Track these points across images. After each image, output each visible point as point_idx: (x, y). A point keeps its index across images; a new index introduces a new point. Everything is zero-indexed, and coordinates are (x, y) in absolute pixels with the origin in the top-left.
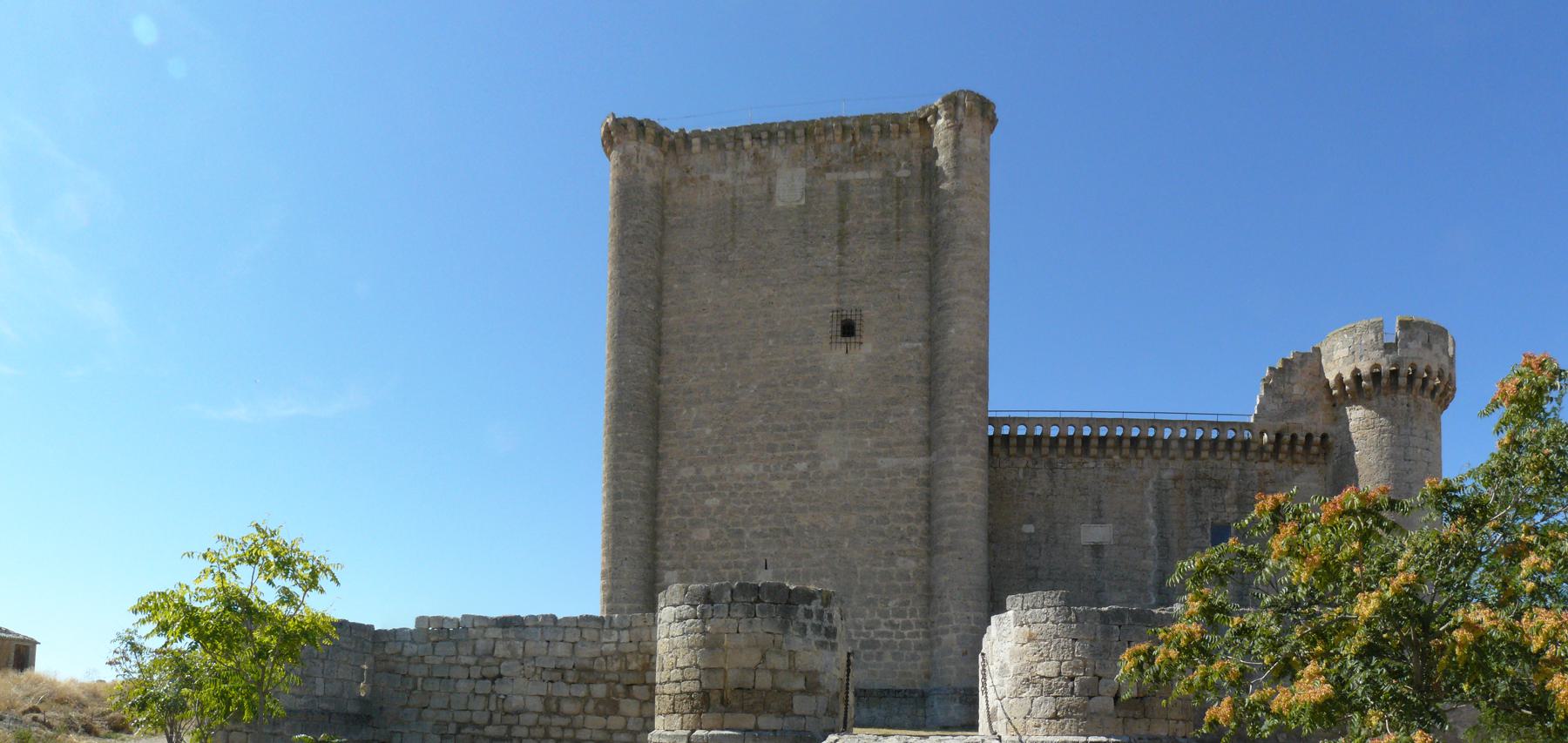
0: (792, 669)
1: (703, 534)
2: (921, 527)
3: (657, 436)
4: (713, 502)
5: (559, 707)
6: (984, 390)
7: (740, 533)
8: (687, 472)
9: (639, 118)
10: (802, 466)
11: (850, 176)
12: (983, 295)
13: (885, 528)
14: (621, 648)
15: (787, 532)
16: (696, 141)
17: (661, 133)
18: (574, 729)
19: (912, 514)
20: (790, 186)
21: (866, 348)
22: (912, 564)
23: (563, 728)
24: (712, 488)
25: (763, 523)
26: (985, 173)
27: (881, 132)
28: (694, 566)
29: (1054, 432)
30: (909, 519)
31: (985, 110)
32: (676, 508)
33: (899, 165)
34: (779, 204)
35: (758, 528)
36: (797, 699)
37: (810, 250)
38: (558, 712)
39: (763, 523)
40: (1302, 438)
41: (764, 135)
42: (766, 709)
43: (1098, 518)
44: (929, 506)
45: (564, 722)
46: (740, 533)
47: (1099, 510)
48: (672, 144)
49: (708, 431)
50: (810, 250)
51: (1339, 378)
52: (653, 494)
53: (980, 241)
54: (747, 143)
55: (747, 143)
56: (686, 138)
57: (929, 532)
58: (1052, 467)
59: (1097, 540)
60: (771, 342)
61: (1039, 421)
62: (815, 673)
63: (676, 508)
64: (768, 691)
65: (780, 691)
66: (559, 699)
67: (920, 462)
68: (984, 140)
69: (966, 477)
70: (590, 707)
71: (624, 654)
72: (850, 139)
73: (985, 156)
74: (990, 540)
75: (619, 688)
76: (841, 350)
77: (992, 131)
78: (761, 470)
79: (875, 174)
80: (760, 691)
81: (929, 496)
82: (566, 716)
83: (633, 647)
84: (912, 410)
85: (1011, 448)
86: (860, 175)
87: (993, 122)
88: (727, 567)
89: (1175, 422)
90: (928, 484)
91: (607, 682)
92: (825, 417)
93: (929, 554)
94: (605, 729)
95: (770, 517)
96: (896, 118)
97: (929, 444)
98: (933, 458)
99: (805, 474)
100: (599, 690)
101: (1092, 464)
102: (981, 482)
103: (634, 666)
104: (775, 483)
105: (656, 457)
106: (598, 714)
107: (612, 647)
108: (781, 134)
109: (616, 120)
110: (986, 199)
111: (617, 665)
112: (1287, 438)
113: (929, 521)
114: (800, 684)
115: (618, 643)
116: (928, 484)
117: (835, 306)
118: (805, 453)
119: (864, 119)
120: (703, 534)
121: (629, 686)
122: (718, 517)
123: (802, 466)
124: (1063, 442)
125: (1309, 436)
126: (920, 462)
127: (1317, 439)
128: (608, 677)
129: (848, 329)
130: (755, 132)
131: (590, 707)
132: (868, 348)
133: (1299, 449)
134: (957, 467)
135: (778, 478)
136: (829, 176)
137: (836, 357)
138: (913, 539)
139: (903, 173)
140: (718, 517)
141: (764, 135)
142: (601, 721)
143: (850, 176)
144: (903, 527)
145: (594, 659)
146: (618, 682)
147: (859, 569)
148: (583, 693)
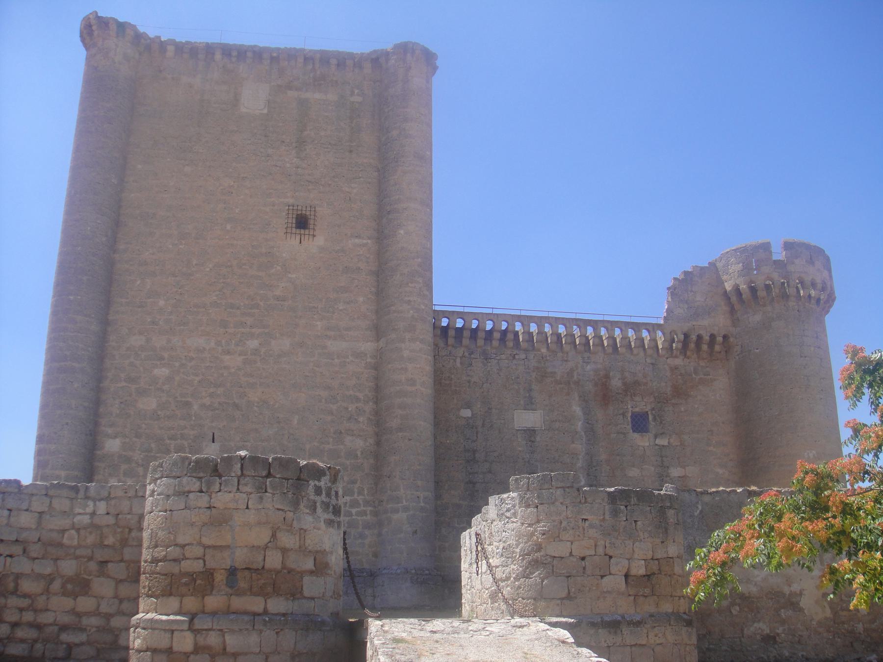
0: (303, 550)
1: (149, 404)
2: (369, 407)
3: (108, 304)
4: (162, 372)
5: (17, 585)
6: (428, 285)
7: (188, 404)
8: (137, 341)
9: (121, 20)
10: (253, 344)
11: (308, 95)
12: (428, 204)
13: (334, 407)
14: (97, 521)
15: (236, 406)
16: (171, 48)
17: (139, 37)
18: (35, 611)
19: (361, 396)
20: (254, 98)
21: (320, 240)
22: (359, 444)
23: (21, 610)
24: (162, 358)
25: (211, 395)
26: (428, 105)
27: (338, 65)
28: (138, 436)
29: (489, 326)
30: (358, 399)
31: (429, 58)
32: (123, 375)
33: (352, 94)
34: (244, 110)
35: (207, 401)
36: (307, 579)
37: (270, 151)
38: (15, 592)
39: (211, 395)
40: (707, 338)
41: (234, 53)
42: (276, 591)
43: (530, 404)
44: (377, 389)
45: (25, 603)
46: (188, 404)
47: (531, 398)
48: (147, 48)
49: (162, 303)
50: (270, 151)
51: (737, 290)
52: (100, 356)
53: (425, 159)
54: (218, 56)
55: (218, 56)
56: (162, 46)
57: (377, 413)
58: (486, 357)
59: (529, 425)
60: (228, 227)
61: (475, 316)
62: (324, 552)
63: (123, 375)
64: (278, 572)
65: (290, 571)
66: (18, 577)
67: (368, 347)
68: (428, 81)
69: (414, 365)
70: (56, 586)
71: (97, 527)
72: (310, 67)
73: (428, 92)
74: (436, 424)
75: (93, 566)
76: (294, 241)
77: (433, 75)
78: (213, 344)
79: (332, 97)
80: (270, 571)
81: (377, 378)
82: (25, 596)
83: (111, 520)
84: (361, 299)
85: (458, 339)
86: (317, 96)
87: (435, 68)
88: (173, 438)
89: (596, 322)
90: (376, 367)
91: (77, 558)
92: (278, 298)
93: (377, 434)
94: (73, 612)
95: (220, 391)
96: (351, 56)
97: (378, 331)
98: (382, 343)
99: (256, 352)
100: (68, 567)
101: (523, 356)
102: (429, 368)
103: (110, 541)
104: (228, 357)
105: (105, 323)
106: (65, 593)
107: (86, 519)
108: (249, 54)
109: (99, 18)
110: (430, 125)
111: (91, 539)
112: (694, 337)
113: (376, 403)
114: (309, 565)
115: (93, 514)
116: (376, 367)
117: (291, 201)
118: (256, 331)
119: (323, 52)
120: (149, 404)
121: (103, 563)
122: (166, 387)
123: (253, 344)
124: (497, 335)
125: (713, 337)
126: (368, 347)
127: (720, 339)
128: (78, 552)
129: (302, 223)
130: (227, 50)
131: (56, 586)
132: (320, 240)
133: (705, 347)
134: (406, 353)
135: (228, 353)
136: (292, 94)
137: (291, 246)
138: (361, 419)
139: (357, 99)
140: (166, 387)
141: (234, 53)
142: (68, 603)
143: (308, 95)
144: (352, 407)
145: (63, 531)
146: (91, 559)
147: (308, 447)
148: (48, 570)
